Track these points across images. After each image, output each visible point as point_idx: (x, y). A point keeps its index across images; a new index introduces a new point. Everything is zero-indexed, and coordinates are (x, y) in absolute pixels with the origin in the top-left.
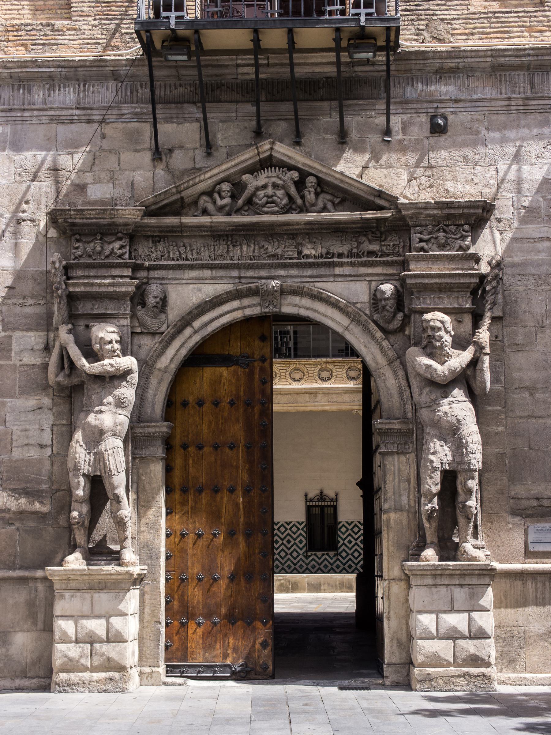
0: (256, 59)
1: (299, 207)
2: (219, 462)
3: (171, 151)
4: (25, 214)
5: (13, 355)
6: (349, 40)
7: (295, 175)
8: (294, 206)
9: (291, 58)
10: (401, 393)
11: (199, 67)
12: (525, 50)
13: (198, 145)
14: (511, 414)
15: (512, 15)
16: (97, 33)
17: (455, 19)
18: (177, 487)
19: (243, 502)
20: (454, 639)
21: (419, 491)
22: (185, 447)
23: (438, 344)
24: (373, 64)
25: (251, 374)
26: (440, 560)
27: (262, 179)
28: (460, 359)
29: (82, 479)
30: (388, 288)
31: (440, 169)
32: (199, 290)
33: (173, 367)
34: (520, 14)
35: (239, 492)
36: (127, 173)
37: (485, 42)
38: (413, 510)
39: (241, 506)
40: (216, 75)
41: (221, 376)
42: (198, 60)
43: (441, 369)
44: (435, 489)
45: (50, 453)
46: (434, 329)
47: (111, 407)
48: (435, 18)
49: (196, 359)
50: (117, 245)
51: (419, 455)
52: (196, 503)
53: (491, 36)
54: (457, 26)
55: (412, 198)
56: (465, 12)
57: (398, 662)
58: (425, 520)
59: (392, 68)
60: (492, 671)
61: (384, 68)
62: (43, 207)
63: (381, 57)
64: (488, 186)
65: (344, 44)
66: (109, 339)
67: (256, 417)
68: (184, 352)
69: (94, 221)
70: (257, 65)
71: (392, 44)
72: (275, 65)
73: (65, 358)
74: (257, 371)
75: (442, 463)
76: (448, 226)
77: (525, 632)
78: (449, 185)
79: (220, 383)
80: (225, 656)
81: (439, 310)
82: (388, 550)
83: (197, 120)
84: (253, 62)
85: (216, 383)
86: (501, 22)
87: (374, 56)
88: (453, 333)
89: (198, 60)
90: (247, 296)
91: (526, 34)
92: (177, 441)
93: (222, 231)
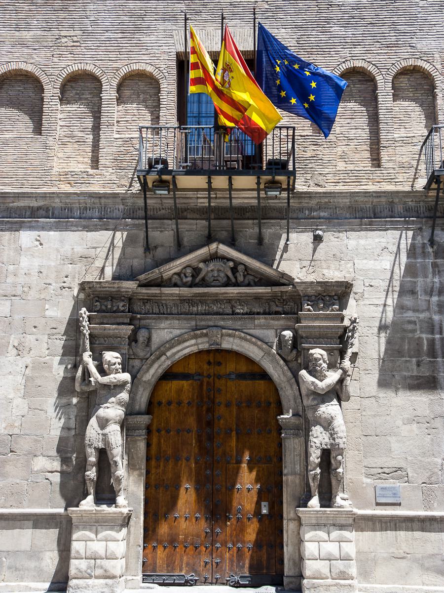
0: (209, 194)
1: (233, 283)
2: (180, 441)
3: (156, 247)
4: (65, 284)
5: (53, 370)
6: (265, 184)
7: (231, 264)
8: (230, 283)
9: (230, 194)
10: (295, 399)
11: (175, 198)
12: (370, 192)
13: (172, 245)
14: (364, 413)
15: (362, 172)
16: (114, 177)
17: (328, 174)
18: (153, 457)
19: (195, 467)
20: (330, 560)
21: (307, 462)
22: (159, 431)
23: (319, 369)
24: (279, 199)
25: (201, 385)
26: (321, 507)
27: (212, 266)
28: (333, 377)
29: (93, 450)
30: (288, 334)
31: (320, 262)
32: (171, 333)
33: (154, 380)
34: (367, 172)
35: (192, 461)
36: (128, 260)
37: (346, 187)
38: (302, 474)
39: (193, 470)
40: (185, 203)
41: (183, 385)
42: (174, 194)
43: (322, 385)
44: (318, 461)
45: (74, 434)
46: (316, 360)
47: (113, 405)
48: (316, 172)
49: (168, 375)
50: (121, 304)
51: (307, 438)
52: (165, 467)
53: (350, 184)
54: (329, 178)
55: (302, 279)
56: (334, 170)
57: (293, 575)
58: (311, 481)
59: (291, 201)
60: (354, 582)
61: (286, 201)
62: (76, 280)
63: (284, 195)
64: (349, 272)
65: (262, 186)
66: (114, 362)
67: (204, 413)
68: (160, 371)
69: (107, 289)
70: (209, 198)
71: (291, 187)
72: (220, 198)
73: (86, 374)
74: (205, 384)
75: (321, 444)
76: (324, 296)
77: (375, 556)
78: (325, 271)
79: (182, 391)
80: (181, 570)
81: (319, 347)
82: (287, 500)
83: (172, 230)
84: (207, 196)
85: (180, 391)
86: (356, 176)
87: (280, 194)
88: (328, 362)
89: (174, 194)
90: (200, 337)
91: (371, 183)
92: (154, 427)
93: (185, 297)
